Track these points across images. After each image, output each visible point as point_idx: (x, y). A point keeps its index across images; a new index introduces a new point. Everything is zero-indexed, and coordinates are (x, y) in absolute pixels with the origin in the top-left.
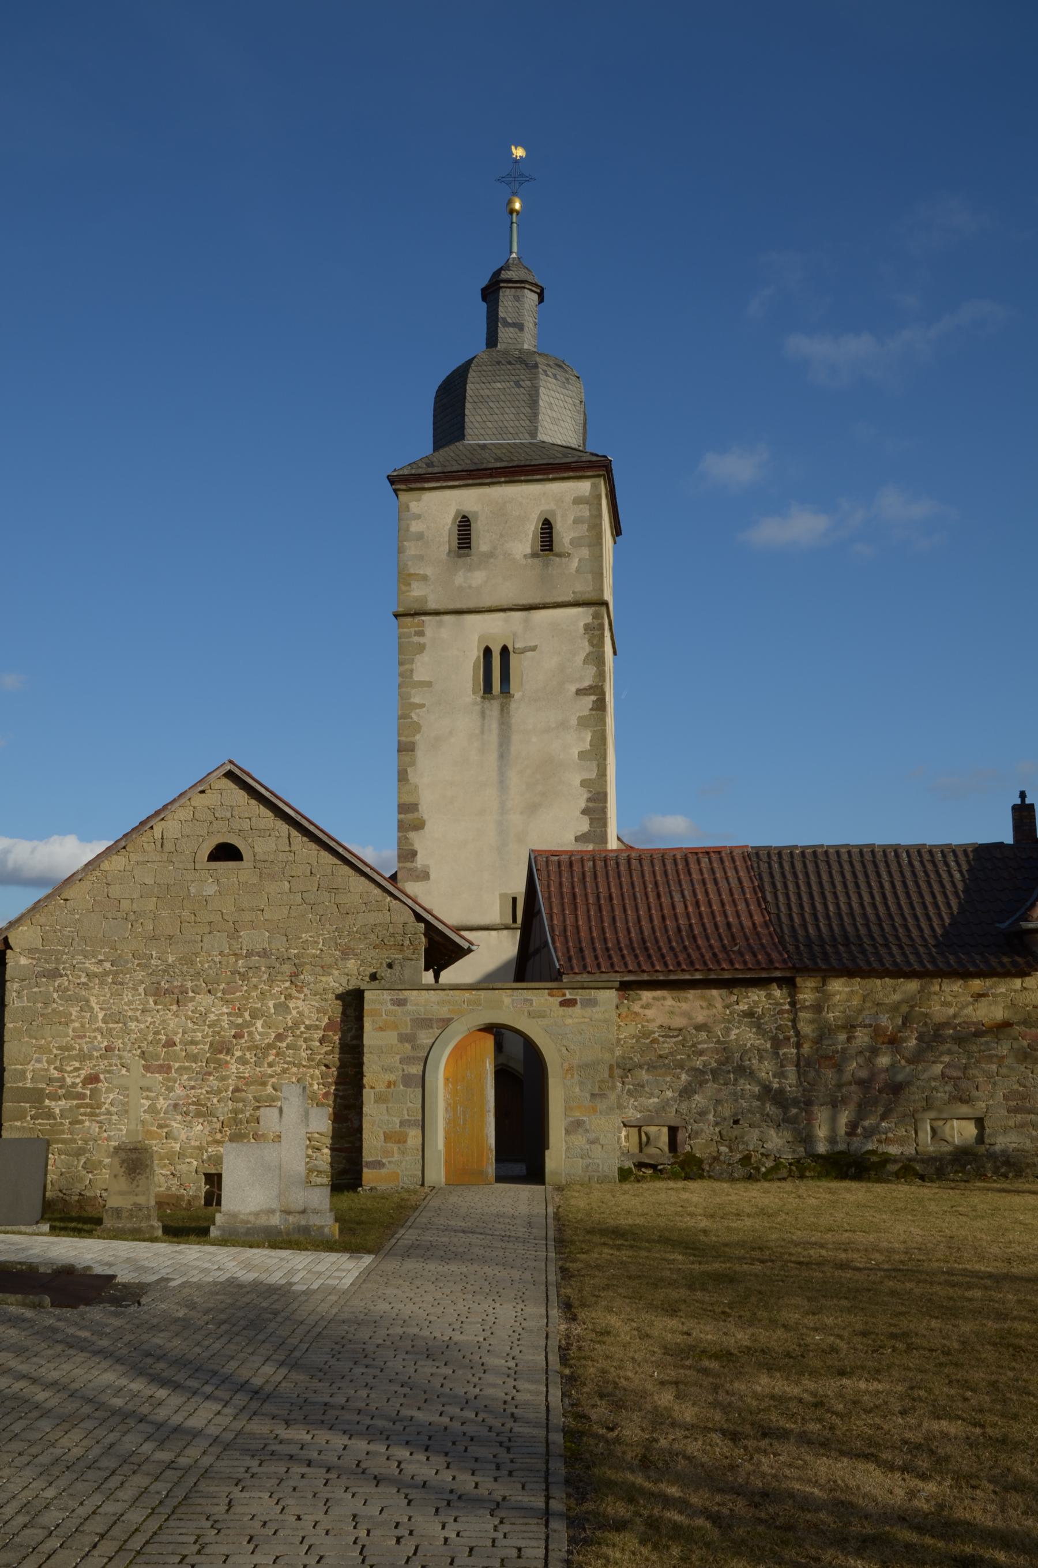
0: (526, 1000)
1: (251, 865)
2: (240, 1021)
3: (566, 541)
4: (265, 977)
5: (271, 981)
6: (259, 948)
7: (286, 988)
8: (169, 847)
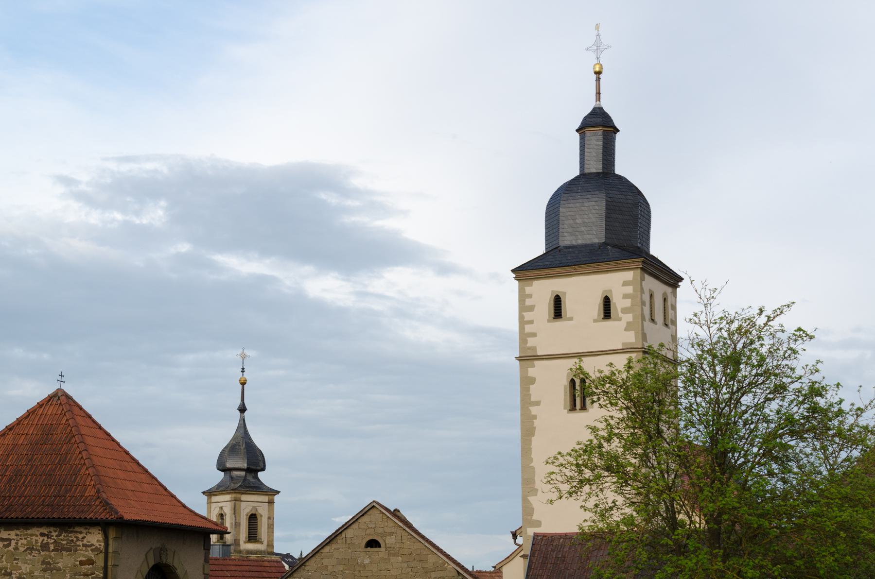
1: (384, 549)
3: (619, 310)
8: (349, 541)
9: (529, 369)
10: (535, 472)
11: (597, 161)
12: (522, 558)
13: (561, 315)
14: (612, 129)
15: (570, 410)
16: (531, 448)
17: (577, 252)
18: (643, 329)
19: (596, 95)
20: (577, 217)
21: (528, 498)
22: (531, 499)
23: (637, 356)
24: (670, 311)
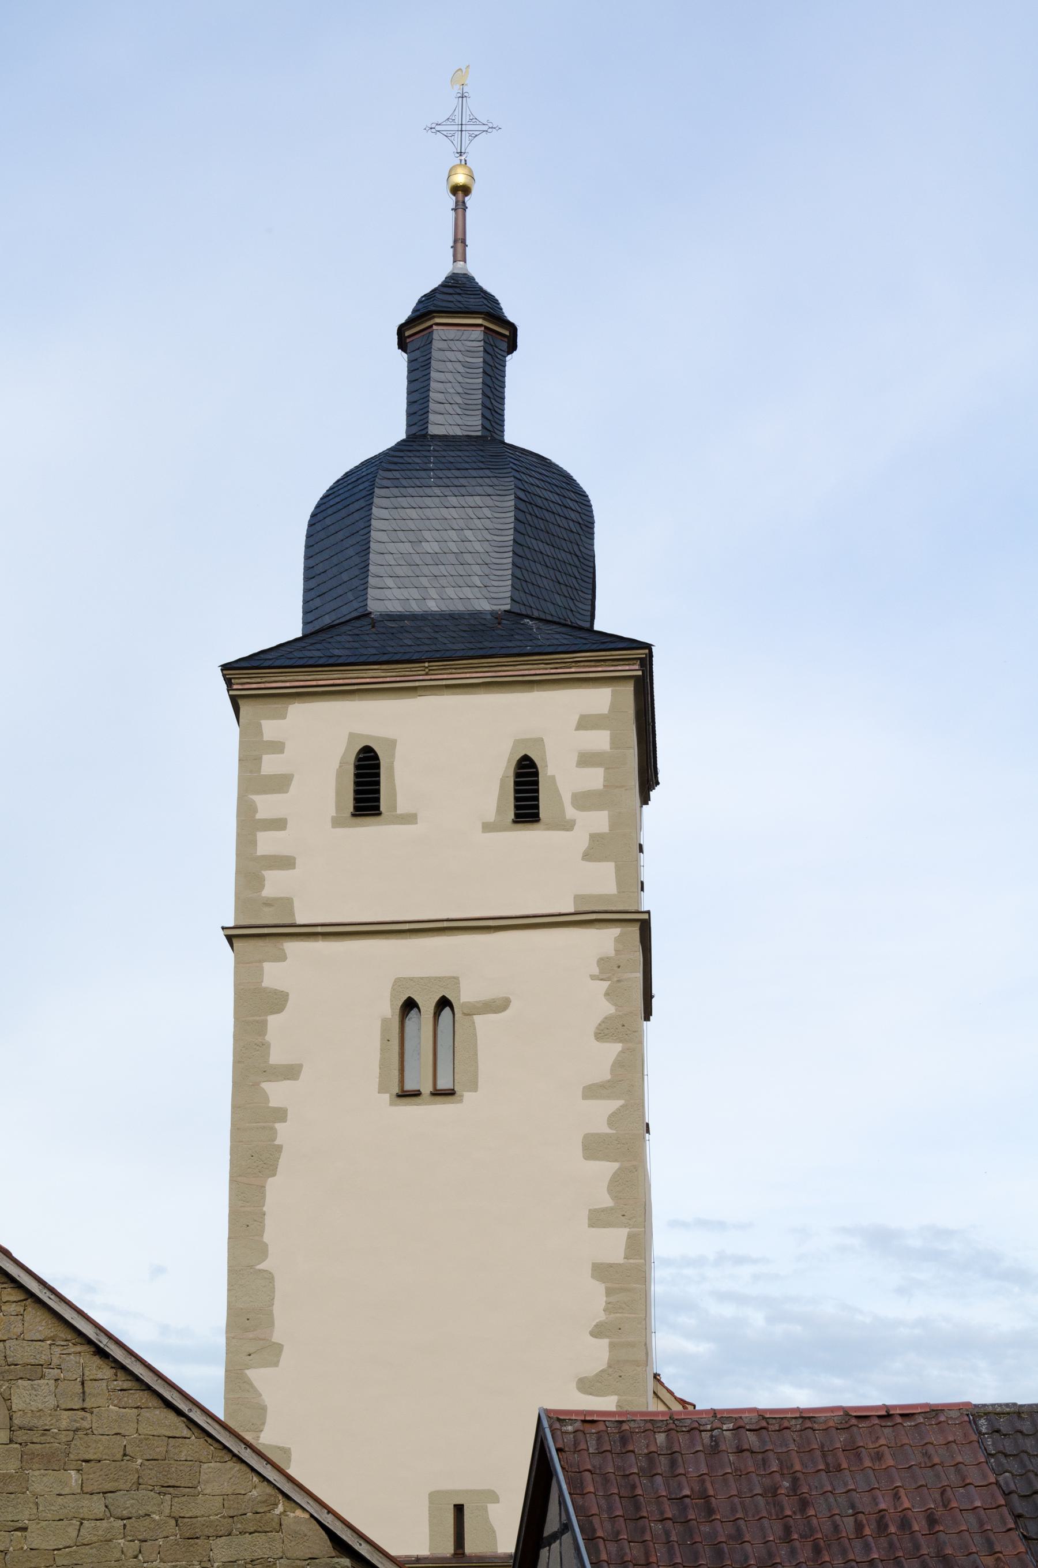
9: (267, 966)
10: (273, 1290)
11: (466, 407)
13: (378, 808)
15: (399, 1096)
20: (427, 535)
21: (247, 1372)
22: (257, 1375)
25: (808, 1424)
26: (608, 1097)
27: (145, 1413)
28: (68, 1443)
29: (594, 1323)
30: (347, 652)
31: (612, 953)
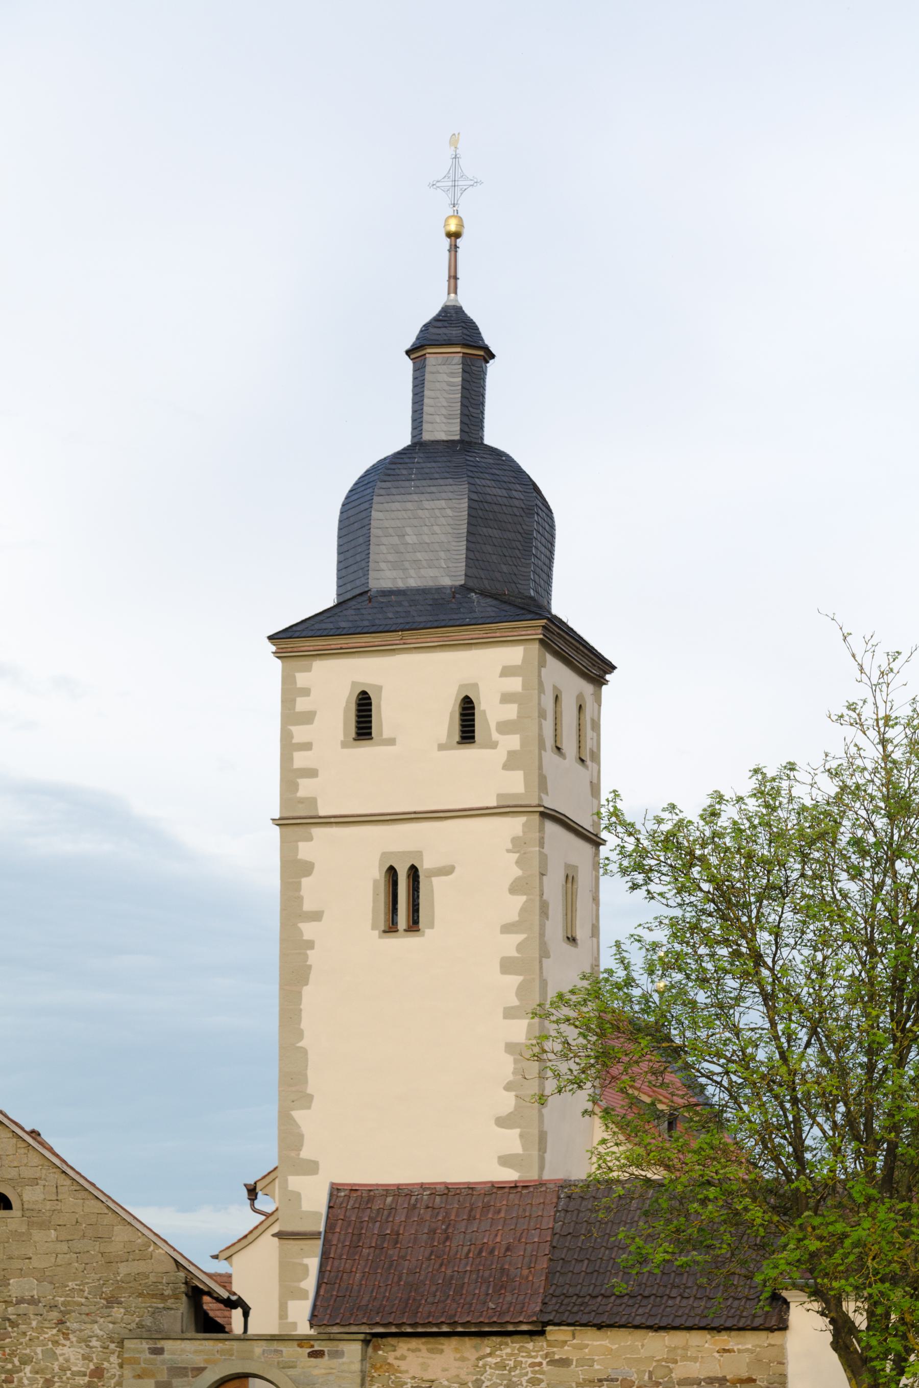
0: (276, 1351)
1: (19, 1214)
2: (10, 1366)
4: (34, 1324)
5: (41, 1329)
6: (27, 1295)
7: (53, 1335)
9: (302, 845)
10: (306, 1060)
11: (448, 417)
12: (276, 1239)
13: (370, 734)
14: (482, 353)
15: (385, 932)
16: (301, 1010)
17: (406, 604)
18: (540, 767)
19: (449, 281)
20: (408, 530)
22: (298, 1115)
23: (527, 821)
24: (589, 733)
25: (470, 1192)
26: (516, 933)
27: (87, 1202)
28: (50, 1217)
29: (506, 1082)
30: (350, 624)
31: (521, 834)
